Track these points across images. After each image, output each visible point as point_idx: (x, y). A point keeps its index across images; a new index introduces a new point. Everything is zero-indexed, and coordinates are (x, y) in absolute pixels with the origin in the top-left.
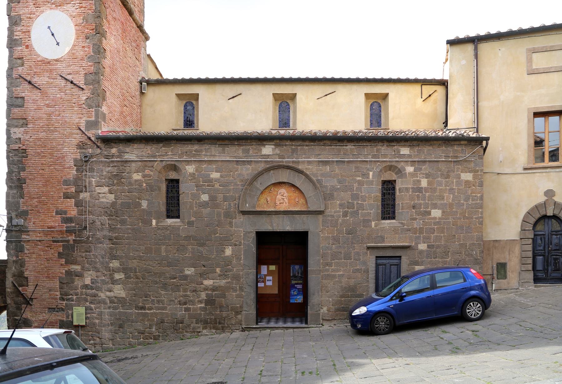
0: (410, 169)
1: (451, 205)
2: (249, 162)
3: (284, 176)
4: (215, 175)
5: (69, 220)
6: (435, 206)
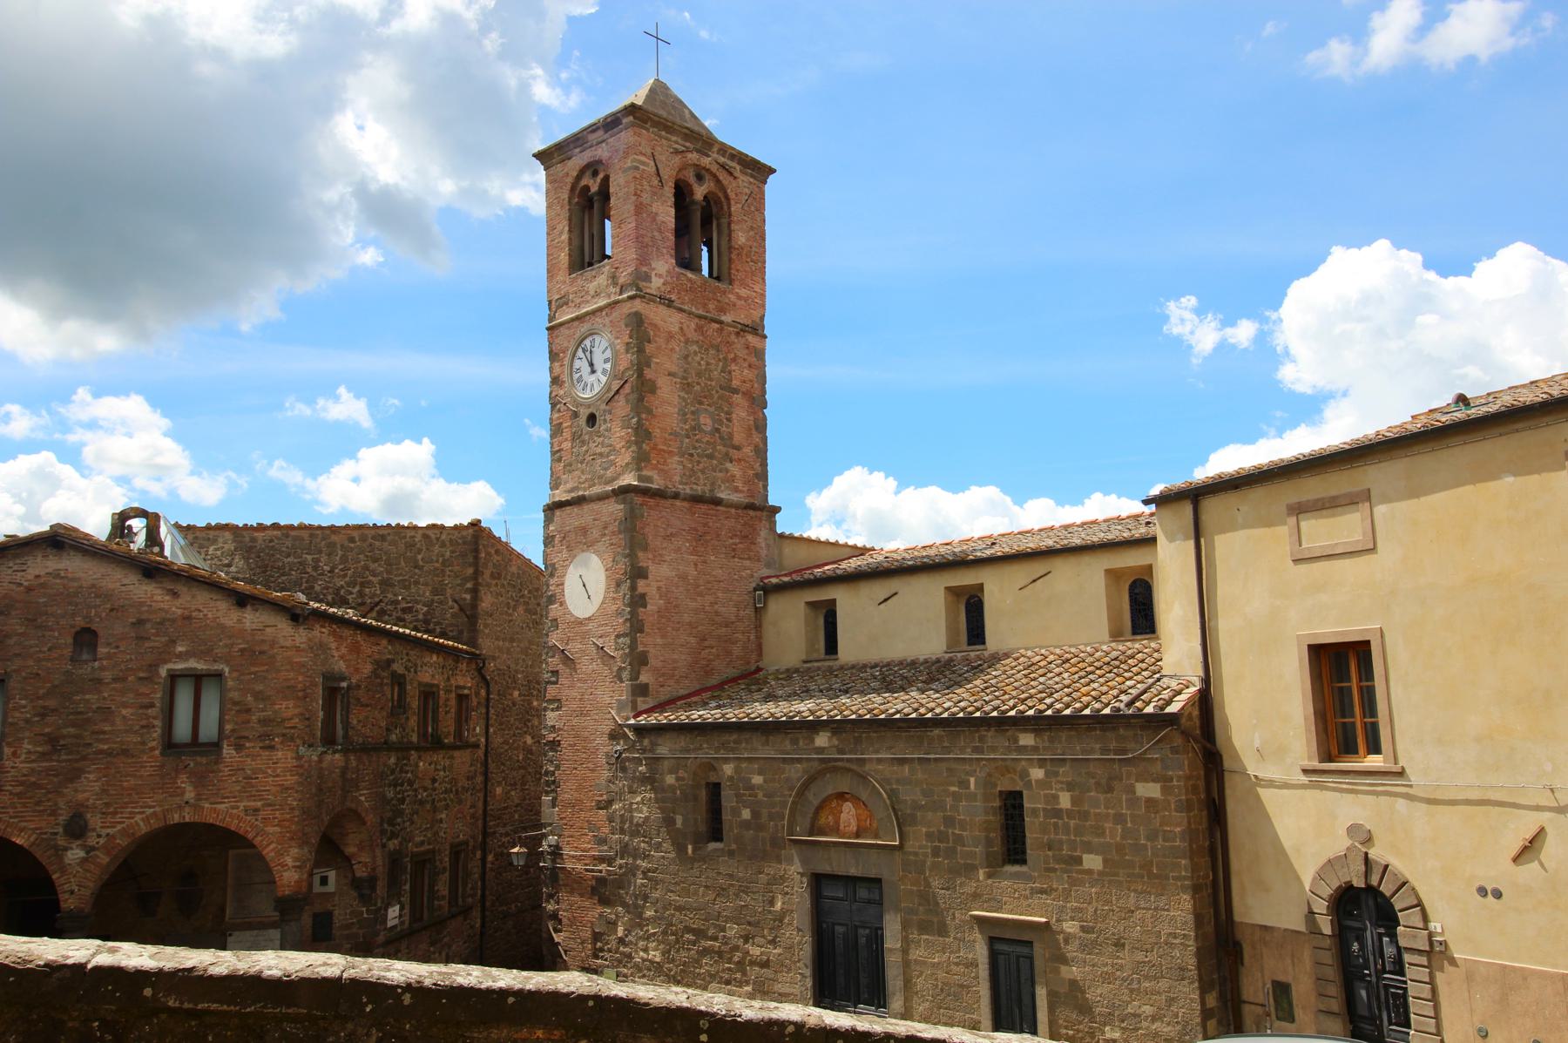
0: (1037, 773)
1: (1120, 848)
2: (799, 760)
3: (844, 784)
4: (757, 780)
5: (602, 841)
6: (1089, 848)
